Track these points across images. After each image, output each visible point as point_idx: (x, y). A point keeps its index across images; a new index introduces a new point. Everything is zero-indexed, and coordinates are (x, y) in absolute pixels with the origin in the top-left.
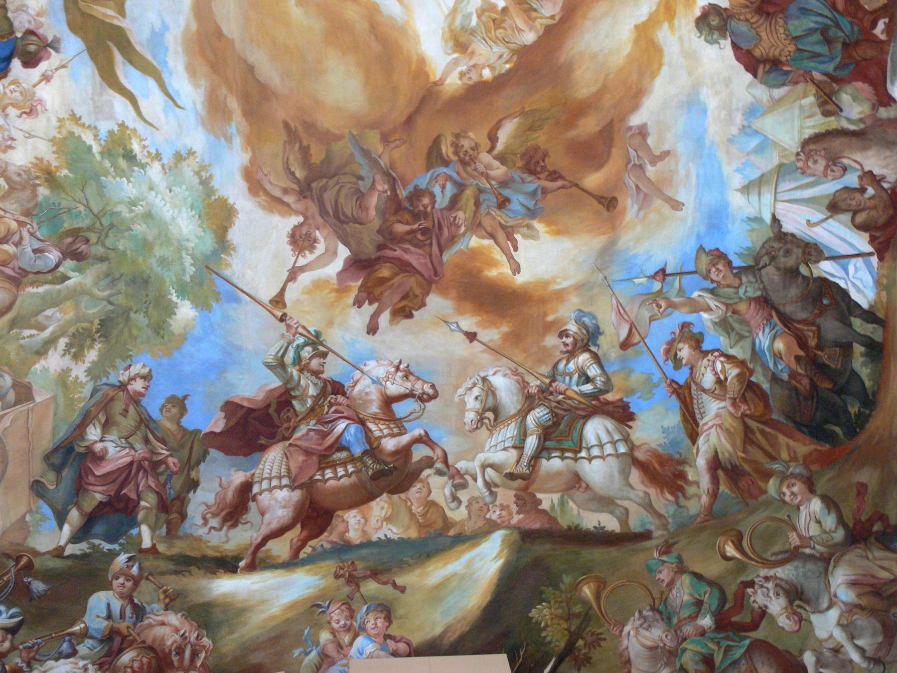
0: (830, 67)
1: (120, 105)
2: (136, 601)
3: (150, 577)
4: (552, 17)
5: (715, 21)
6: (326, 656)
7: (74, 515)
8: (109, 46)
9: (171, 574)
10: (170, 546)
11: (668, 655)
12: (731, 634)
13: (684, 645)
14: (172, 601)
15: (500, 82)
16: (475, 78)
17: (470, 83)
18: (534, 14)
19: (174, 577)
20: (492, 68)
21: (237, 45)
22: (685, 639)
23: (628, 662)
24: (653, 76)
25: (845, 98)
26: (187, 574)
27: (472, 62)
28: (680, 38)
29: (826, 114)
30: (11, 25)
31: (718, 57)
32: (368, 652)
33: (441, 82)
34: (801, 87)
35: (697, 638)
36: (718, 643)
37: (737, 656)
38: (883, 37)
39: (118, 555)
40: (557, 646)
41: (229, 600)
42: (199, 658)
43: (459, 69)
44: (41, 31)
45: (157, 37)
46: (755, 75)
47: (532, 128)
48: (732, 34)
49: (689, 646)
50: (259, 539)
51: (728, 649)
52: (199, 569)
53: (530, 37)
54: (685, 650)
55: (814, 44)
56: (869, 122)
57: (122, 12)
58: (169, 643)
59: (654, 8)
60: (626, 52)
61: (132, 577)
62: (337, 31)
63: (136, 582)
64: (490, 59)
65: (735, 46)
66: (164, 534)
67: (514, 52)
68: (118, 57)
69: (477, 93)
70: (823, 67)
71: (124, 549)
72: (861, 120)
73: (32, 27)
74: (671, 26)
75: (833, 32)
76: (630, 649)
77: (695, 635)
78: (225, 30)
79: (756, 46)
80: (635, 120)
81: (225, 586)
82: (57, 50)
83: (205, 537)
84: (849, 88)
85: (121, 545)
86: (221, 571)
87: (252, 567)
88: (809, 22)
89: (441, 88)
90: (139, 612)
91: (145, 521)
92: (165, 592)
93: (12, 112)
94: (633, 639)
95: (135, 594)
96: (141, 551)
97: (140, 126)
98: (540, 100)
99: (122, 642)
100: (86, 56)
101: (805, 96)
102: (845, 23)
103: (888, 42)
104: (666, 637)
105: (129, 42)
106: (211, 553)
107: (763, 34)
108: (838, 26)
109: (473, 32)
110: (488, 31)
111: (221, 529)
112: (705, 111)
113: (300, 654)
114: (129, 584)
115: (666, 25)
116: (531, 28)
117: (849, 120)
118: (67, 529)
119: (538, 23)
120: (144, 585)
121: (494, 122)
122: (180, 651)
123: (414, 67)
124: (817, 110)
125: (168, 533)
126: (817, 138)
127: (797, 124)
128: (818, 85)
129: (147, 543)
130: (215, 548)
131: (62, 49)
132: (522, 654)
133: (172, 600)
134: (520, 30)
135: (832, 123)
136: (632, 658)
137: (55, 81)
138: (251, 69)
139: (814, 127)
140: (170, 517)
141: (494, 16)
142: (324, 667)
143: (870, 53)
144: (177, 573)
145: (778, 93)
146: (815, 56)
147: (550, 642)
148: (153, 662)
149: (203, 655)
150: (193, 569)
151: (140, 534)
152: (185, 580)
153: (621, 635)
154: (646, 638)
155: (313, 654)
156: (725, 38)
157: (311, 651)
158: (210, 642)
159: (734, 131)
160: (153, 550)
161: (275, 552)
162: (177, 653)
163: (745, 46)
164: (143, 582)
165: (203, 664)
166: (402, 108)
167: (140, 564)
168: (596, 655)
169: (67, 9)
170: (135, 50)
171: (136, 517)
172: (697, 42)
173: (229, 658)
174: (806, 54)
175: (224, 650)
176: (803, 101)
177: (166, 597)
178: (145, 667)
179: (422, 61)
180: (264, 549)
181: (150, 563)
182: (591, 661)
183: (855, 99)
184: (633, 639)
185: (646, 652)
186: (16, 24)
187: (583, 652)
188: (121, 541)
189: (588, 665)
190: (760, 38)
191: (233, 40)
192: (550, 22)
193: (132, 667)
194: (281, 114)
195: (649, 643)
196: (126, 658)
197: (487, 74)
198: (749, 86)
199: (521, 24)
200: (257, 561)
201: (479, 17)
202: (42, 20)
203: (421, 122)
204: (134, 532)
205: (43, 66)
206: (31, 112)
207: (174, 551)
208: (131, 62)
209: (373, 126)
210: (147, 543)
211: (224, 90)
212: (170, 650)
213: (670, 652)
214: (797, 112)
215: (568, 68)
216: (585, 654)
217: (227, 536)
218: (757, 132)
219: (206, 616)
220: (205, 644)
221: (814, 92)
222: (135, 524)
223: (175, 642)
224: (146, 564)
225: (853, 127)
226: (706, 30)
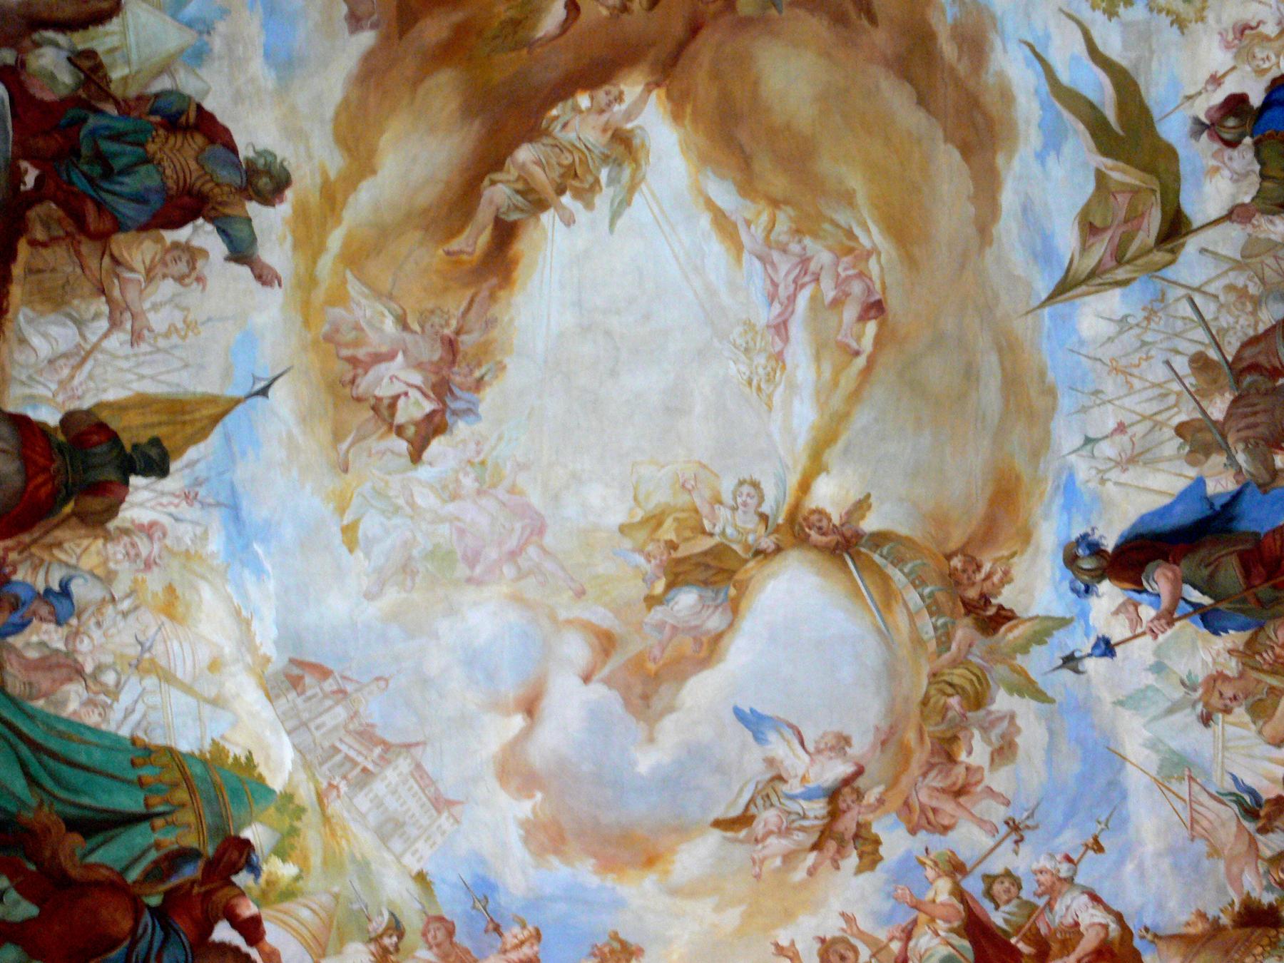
0: (93, 121)
1: (1112, 43)
4: (493, 183)
5: (263, 182)
8: (1122, 127)
15: (564, 89)
16: (601, 94)
17: (607, 87)
18: (520, 186)
20: (577, 110)
21: (940, 134)
24: (346, 102)
25: (66, 77)
27: (605, 117)
28: (311, 158)
29: (91, 54)
30: (1257, 154)
31: (255, 132)
33: (649, 88)
34: (132, 92)
38: (24, 164)
43: (624, 106)
44: (1217, 146)
45: (1053, 142)
46: (199, 108)
47: (516, 24)
48: (237, 165)
53: (525, 154)
55: (122, 154)
56: (27, 43)
57: (1100, 177)
59: (351, 199)
60: (387, 136)
62: (797, 156)
64: (579, 122)
65: (233, 149)
67: (547, 133)
68: (1110, 114)
69: (596, 72)
70: (104, 122)
72: (37, 45)
73: (1228, 152)
74: (324, 174)
75: (97, 171)
78: (956, 155)
79: (202, 150)
80: (367, 38)
82: (1197, 121)
84: (63, 92)
88: (131, 184)
89: (650, 79)
93: (1270, 29)
97: (1086, 14)
98: (505, 65)
100: (1156, 112)
101: (125, 79)
102: (81, 184)
103: (16, 158)
105: (1093, 135)
107: (193, 165)
108: (90, 180)
109: (605, 159)
110: (584, 162)
112: (267, 56)
115: (333, 175)
116: (522, 167)
117: (56, 45)
119: (514, 173)
121: (572, 31)
123: (689, 110)
124: (105, 59)
126: (101, 17)
127: (132, 38)
128: (108, 96)
131: (1189, 123)
134: (538, 163)
135: (81, 41)
137: (1204, 75)
138: (922, 101)
139: (107, 34)
141: (576, 183)
143: (41, 143)
145: (164, 84)
146: (117, 137)
156: (248, 160)
159: (221, 27)
163: (218, 149)
166: (706, 48)
169: (1177, 178)
170: (1088, 125)
172: (286, 153)
174: (129, 139)
176: (126, 71)
179: (677, 117)
183: (53, 77)
186: (1250, 155)
190: (197, 159)
191: (946, 140)
192: (497, 176)
194: (880, 37)
197: (584, 100)
198: (206, 92)
199: (537, 171)
201: (597, 181)
202: (1213, 163)
203: (678, 28)
205: (1219, 97)
206: (1243, 29)
208: (1092, 106)
209: (745, 23)
211: (962, 69)
214: (134, 57)
215: (468, 111)
218: (190, 24)
221: (112, 86)
225: (50, 34)
226: (276, 169)
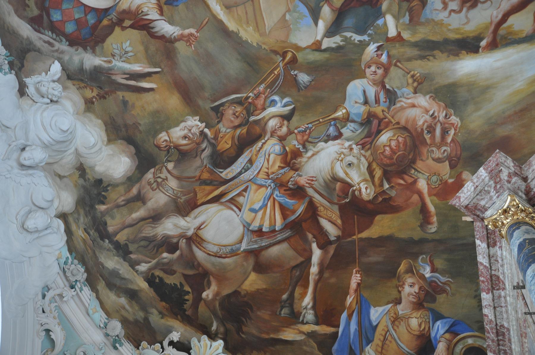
2: (388, 87)
3: (398, 64)
7: (326, 11)
9: (416, 59)
10: (414, 33)
14: (421, 84)
19: (419, 62)
26: (431, 58)
39: (368, 45)
41: (473, 79)
42: (449, 135)
50: (500, 16)
52: (442, 52)
58: (420, 123)
61: (382, 64)
63: (387, 70)
66: (408, 22)
71: (373, 39)
81: (467, 66)
83: (446, 21)
85: (369, 35)
86: (464, 52)
87: (494, 45)
90: (392, 97)
91: (389, 11)
92: (413, 76)
95: (386, 80)
96: (388, 40)
99: (379, 125)
106: (453, 36)
111: (460, 11)
114: (380, 72)
118: (321, 24)
120: (394, 72)
122: (431, 130)
125: (411, 20)
129: (392, 32)
130: (456, 31)
133: (419, 84)
140: (413, 4)
144: (422, 58)
149: (452, 132)
150: (437, 52)
151: (385, 24)
152: (430, 64)
158: (458, 120)
160: (399, 38)
161: (516, 28)
162: (429, 132)
164: (392, 68)
165: (453, 140)
167: (388, 52)
171: (381, 8)
175: (472, 126)
177: (414, 81)
178: (401, 145)
180: (505, 25)
181: (397, 50)
188: (370, 32)
193: (390, 146)
196: (384, 138)
200: (498, 40)
204: (380, 22)
207: (418, 37)
210: (392, 32)
212: (422, 129)
217: (467, 17)
219: (451, 96)
220: (453, 122)
222: (380, 14)
223: (426, 121)
224: (394, 52)
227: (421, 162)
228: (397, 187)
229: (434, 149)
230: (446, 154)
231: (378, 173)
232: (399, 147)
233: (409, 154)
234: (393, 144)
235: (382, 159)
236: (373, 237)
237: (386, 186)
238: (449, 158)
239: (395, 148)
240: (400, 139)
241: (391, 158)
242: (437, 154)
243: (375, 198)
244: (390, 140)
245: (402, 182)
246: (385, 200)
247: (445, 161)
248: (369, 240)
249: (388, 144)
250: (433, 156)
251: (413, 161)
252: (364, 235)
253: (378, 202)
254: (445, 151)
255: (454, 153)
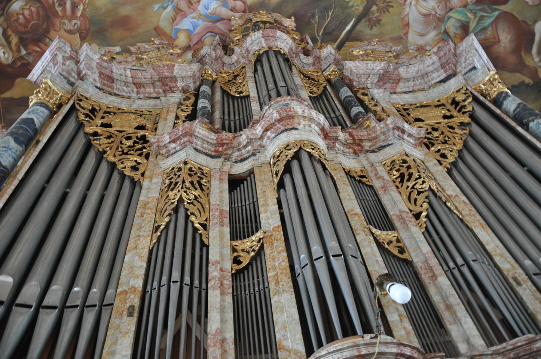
6: (180, 10)
11: (437, 20)
12: (486, 7)
13: (450, 14)
22: (451, 9)
23: (408, 25)
32: (212, 8)
35: (460, 9)
36: (475, 13)
37: (486, 24)
40: (357, 10)
42: (79, 10)
49: (452, 15)
51: (482, 18)
54: (449, 18)
76: (410, 15)
77: (460, 7)
94: (413, 8)
104: (438, 7)
113: (159, 8)
132: (330, 14)
136: (411, 22)
142: (178, 18)
147: (352, 7)
148: (41, 10)
153: (405, 4)
154: (423, 7)
155: (170, 8)
157: (167, 6)
162: (60, 5)
165: (82, 15)
168: (385, 18)
173: (103, 10)
178: (35, 15)
182: (381, 22)
184: (413, 8)
185: (422, 18)
187: (375, 15)
189: (378, 25)
193: (23, 14)
195: (424, 11)
213: (439, 19)
216: (376, 17)
227: (54, 32)
228: (34, 53)
229: (66, 21)
230: (76, 27)
231: (14, 40)
232: (32, 16)
233: (43, 24)
234: (26, 12)
235: (16, 27)
236: (15, 97)
237: (24, 52)
238: (79, 31)
239: (28, 17)
240: (33, 9)
241: (25, 26)
242: (69, 26)
243: (14, 62)
244: (23, 9)
245: (38, 49)
246: (23, 65)
247: (76, 33)
248: (12, 99)
249: (21, 12)
250: (66, 27)
251: (47, 31)
252: (7, 95)
253: (17, 66)
254: (75, 24)
255: (84, 26)
